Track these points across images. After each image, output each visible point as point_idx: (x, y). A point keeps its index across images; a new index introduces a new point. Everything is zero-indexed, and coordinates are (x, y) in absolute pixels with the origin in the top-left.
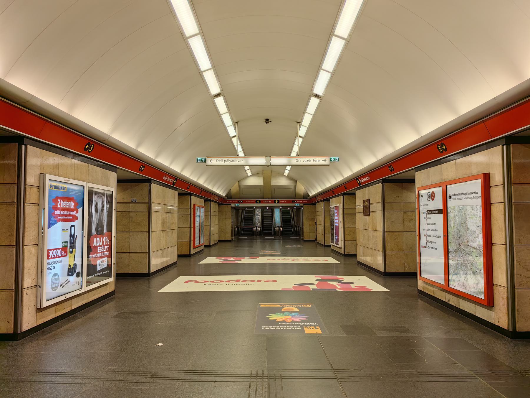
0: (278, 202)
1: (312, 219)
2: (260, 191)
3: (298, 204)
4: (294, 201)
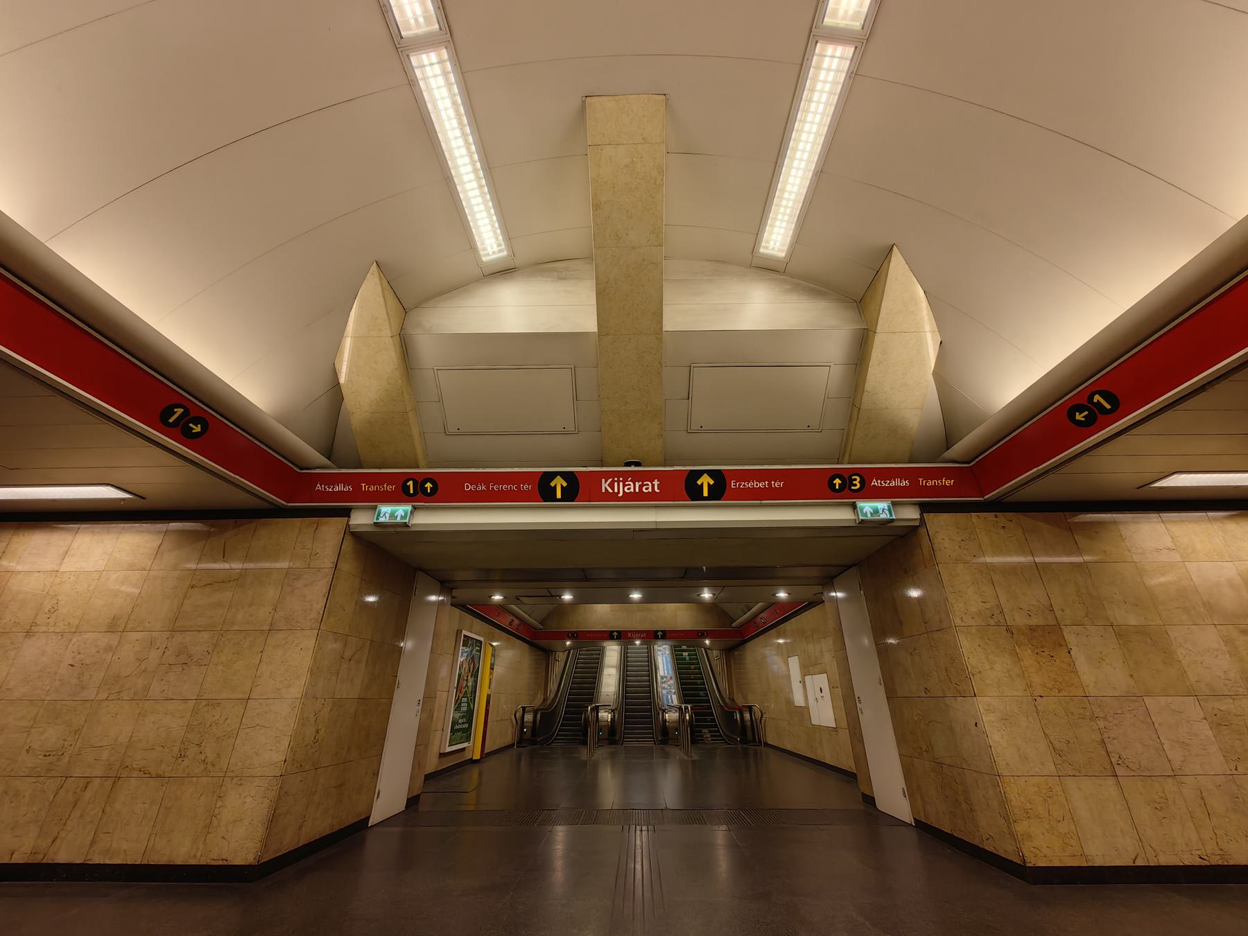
0: (720, 491)
1: (1032, 629)
2: (576, 398)
3: (882, 505)
4: (846, 483)
